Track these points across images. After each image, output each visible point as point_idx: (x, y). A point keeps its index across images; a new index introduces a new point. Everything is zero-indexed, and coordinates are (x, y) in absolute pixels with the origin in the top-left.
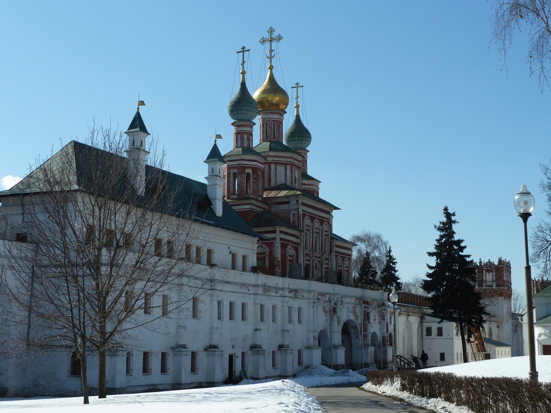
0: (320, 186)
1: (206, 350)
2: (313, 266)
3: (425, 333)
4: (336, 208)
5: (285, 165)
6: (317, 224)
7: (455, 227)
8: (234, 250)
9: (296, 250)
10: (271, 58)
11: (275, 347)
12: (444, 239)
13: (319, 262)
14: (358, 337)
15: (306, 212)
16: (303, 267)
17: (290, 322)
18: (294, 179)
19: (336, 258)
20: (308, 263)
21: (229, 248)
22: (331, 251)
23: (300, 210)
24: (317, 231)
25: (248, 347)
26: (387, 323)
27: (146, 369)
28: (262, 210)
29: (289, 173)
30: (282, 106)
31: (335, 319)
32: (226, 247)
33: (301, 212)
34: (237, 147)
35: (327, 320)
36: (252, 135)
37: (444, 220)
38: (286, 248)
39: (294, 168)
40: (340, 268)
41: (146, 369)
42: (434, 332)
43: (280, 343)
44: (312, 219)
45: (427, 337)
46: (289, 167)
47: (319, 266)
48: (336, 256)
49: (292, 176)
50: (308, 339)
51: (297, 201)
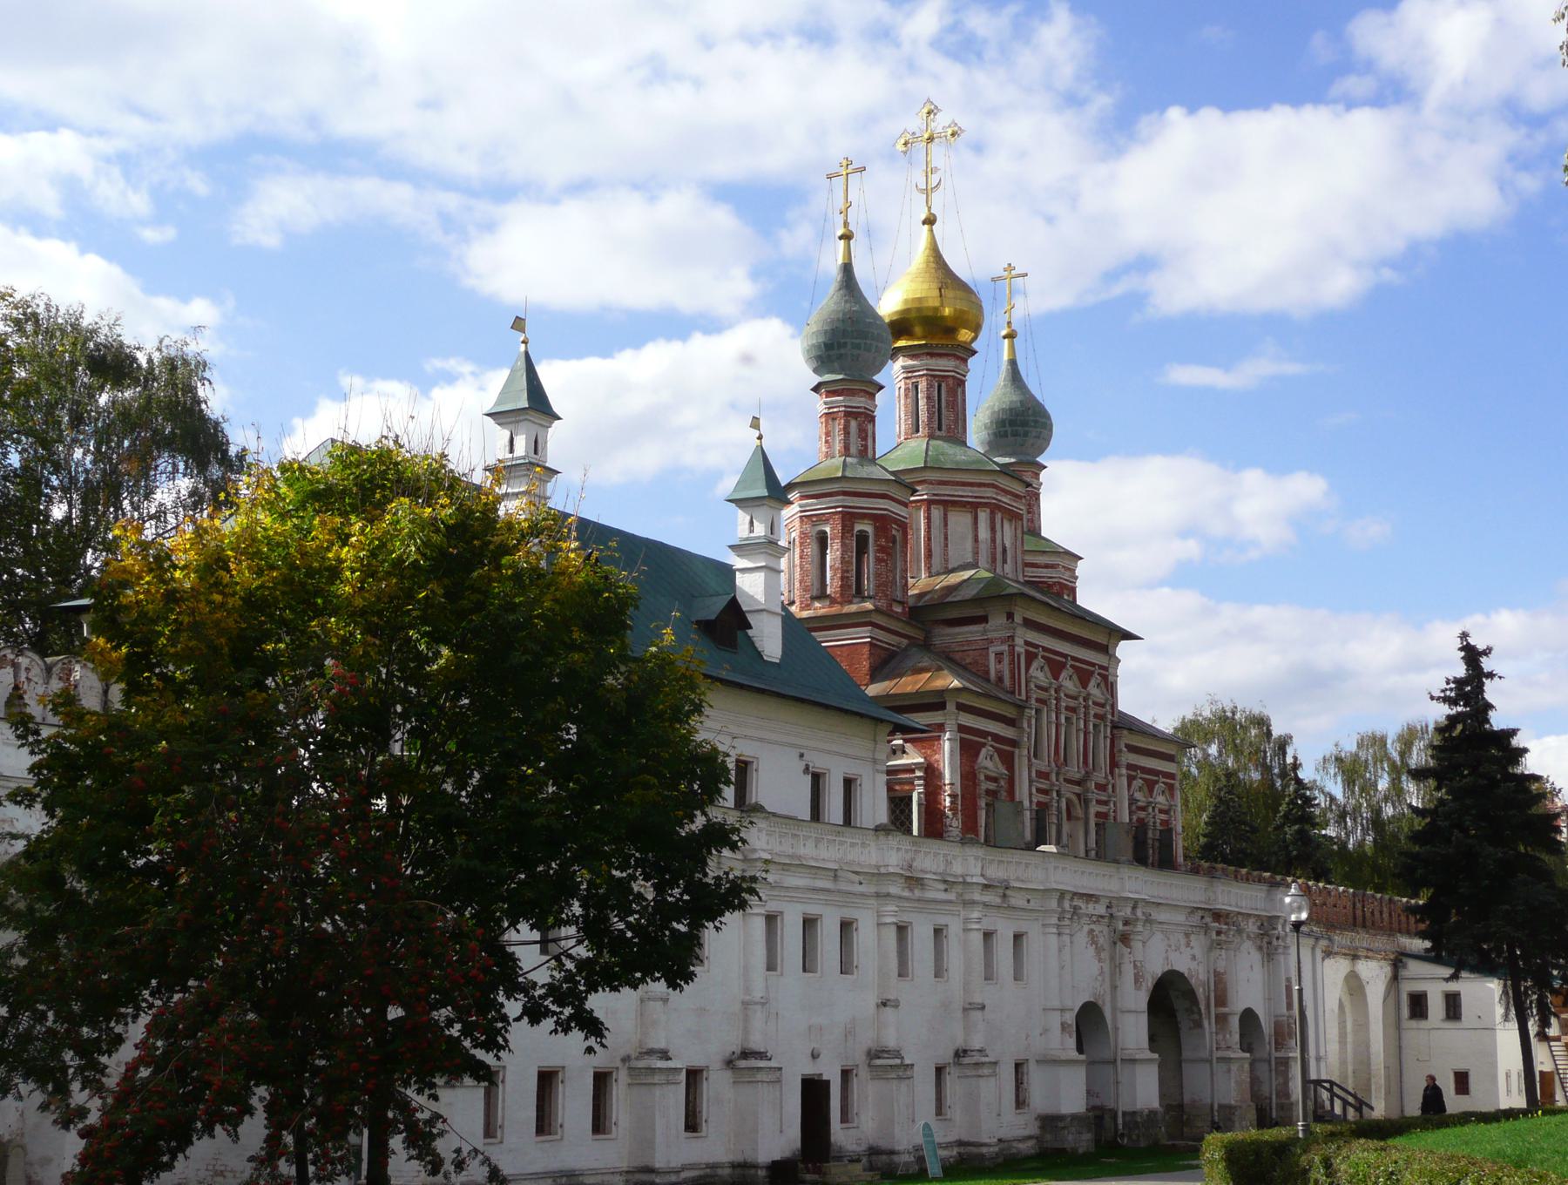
0: (1081, 569)
1: (729, 1063)
2: (1059, 809)
3: (1405, 1012)
4: (1129, 636)
5: (973, 507)
6: (1069, 684)
7: (1491, 691)
8: (819, 762)
9: (1008, 760)
10: (927, 192)
11: (946, 1056)
12: (1460, 727)
13: (1078, 795)
14: (1199, 1025)
15: (1036, 646)
16: (1027, 813)
17: (989, 976)
18: (999, 549)
19: (1129, 786)
20: (1043, 798)
21: (802, 755)
23: (1019, 641)
24: (1072, 703)
25: (859, 1057)
26: (1288, 980)
27: (544, 1123)
28: (905, 642)
29: (984, 533)
30: (964, 335)
31: (1128, 971)
32: (795, 753)
33: (1020, 649)
34: (829, 455)
35: (1102, 973)
36: (872, 419)
37: (1461, 671)
38: (977, 755)
39: (999, 516)
40: (1142, 814)
41: (544, 1123)
42: (1436, 1006)
43: (960, 1043)
44: (1056, 667)
45: (1414, 1023)
46: (983, 516)
47: (1079, 812)
48: (1131, 779)
49: (993, 540)
50: (1045, 1031)
51: (1010, 616)
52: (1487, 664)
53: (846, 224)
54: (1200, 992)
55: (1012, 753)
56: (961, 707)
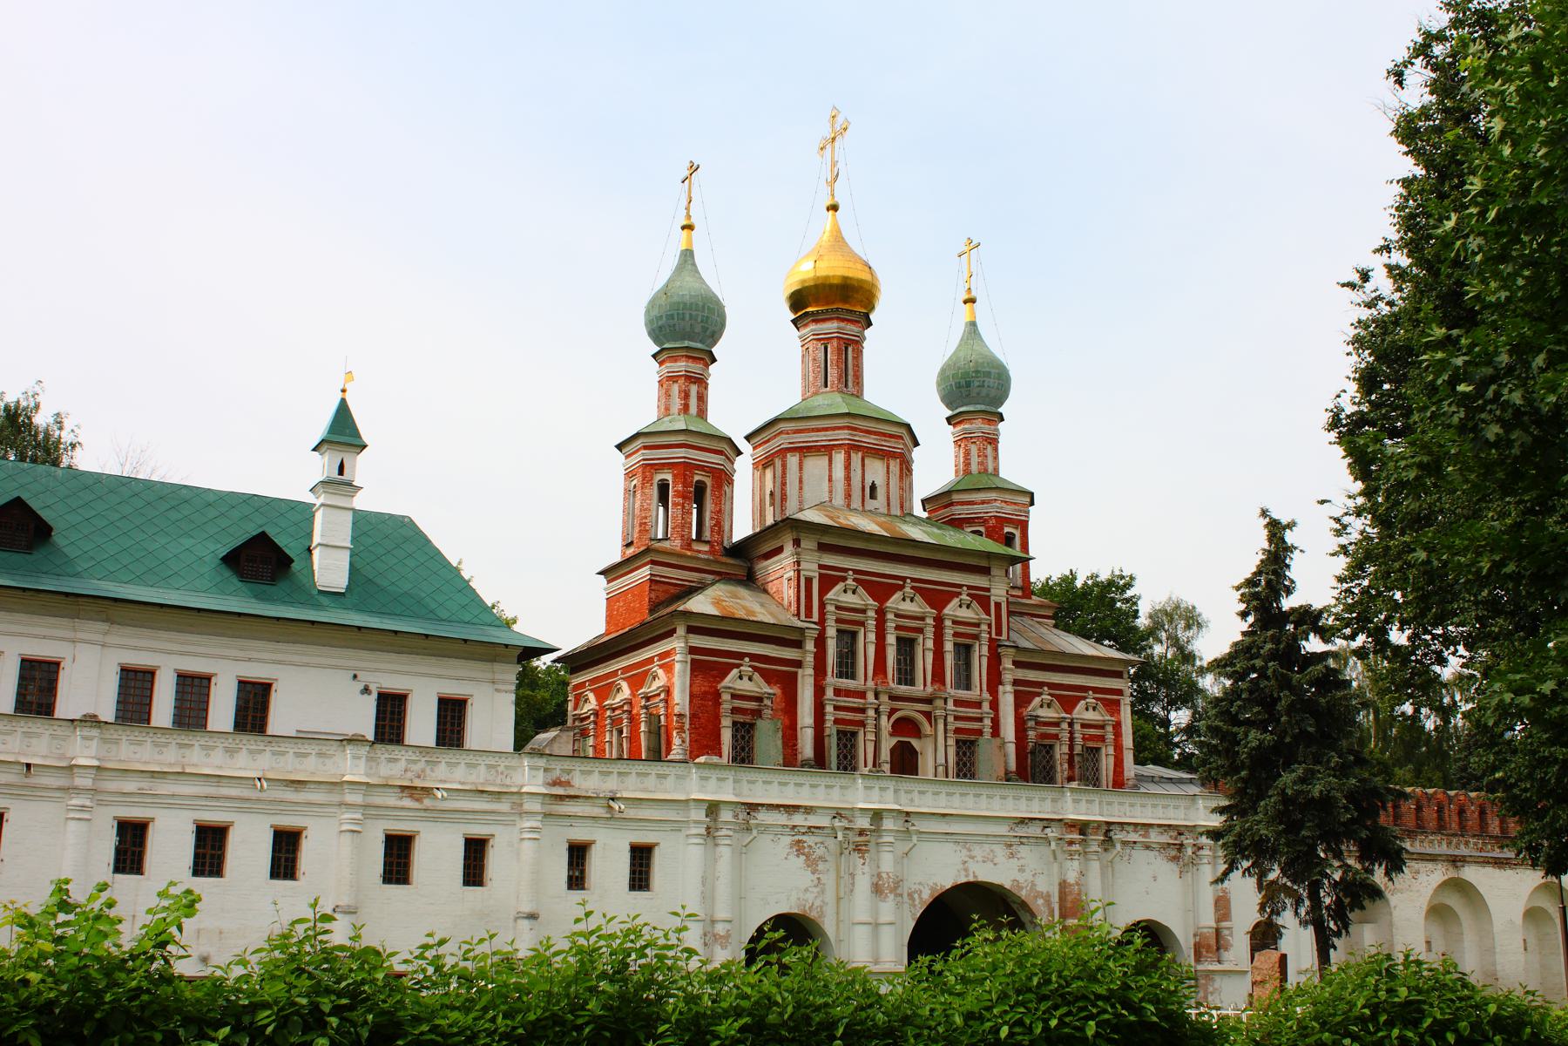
5: (828, 450)
21: (355, 676)
22: (994, 680)
29: (839, 472)
46: (839, 458)
52: (1290, 537)
53: (689, 217)
54: (1038, 905)
55: (796, 674)
56: (691, 630)
